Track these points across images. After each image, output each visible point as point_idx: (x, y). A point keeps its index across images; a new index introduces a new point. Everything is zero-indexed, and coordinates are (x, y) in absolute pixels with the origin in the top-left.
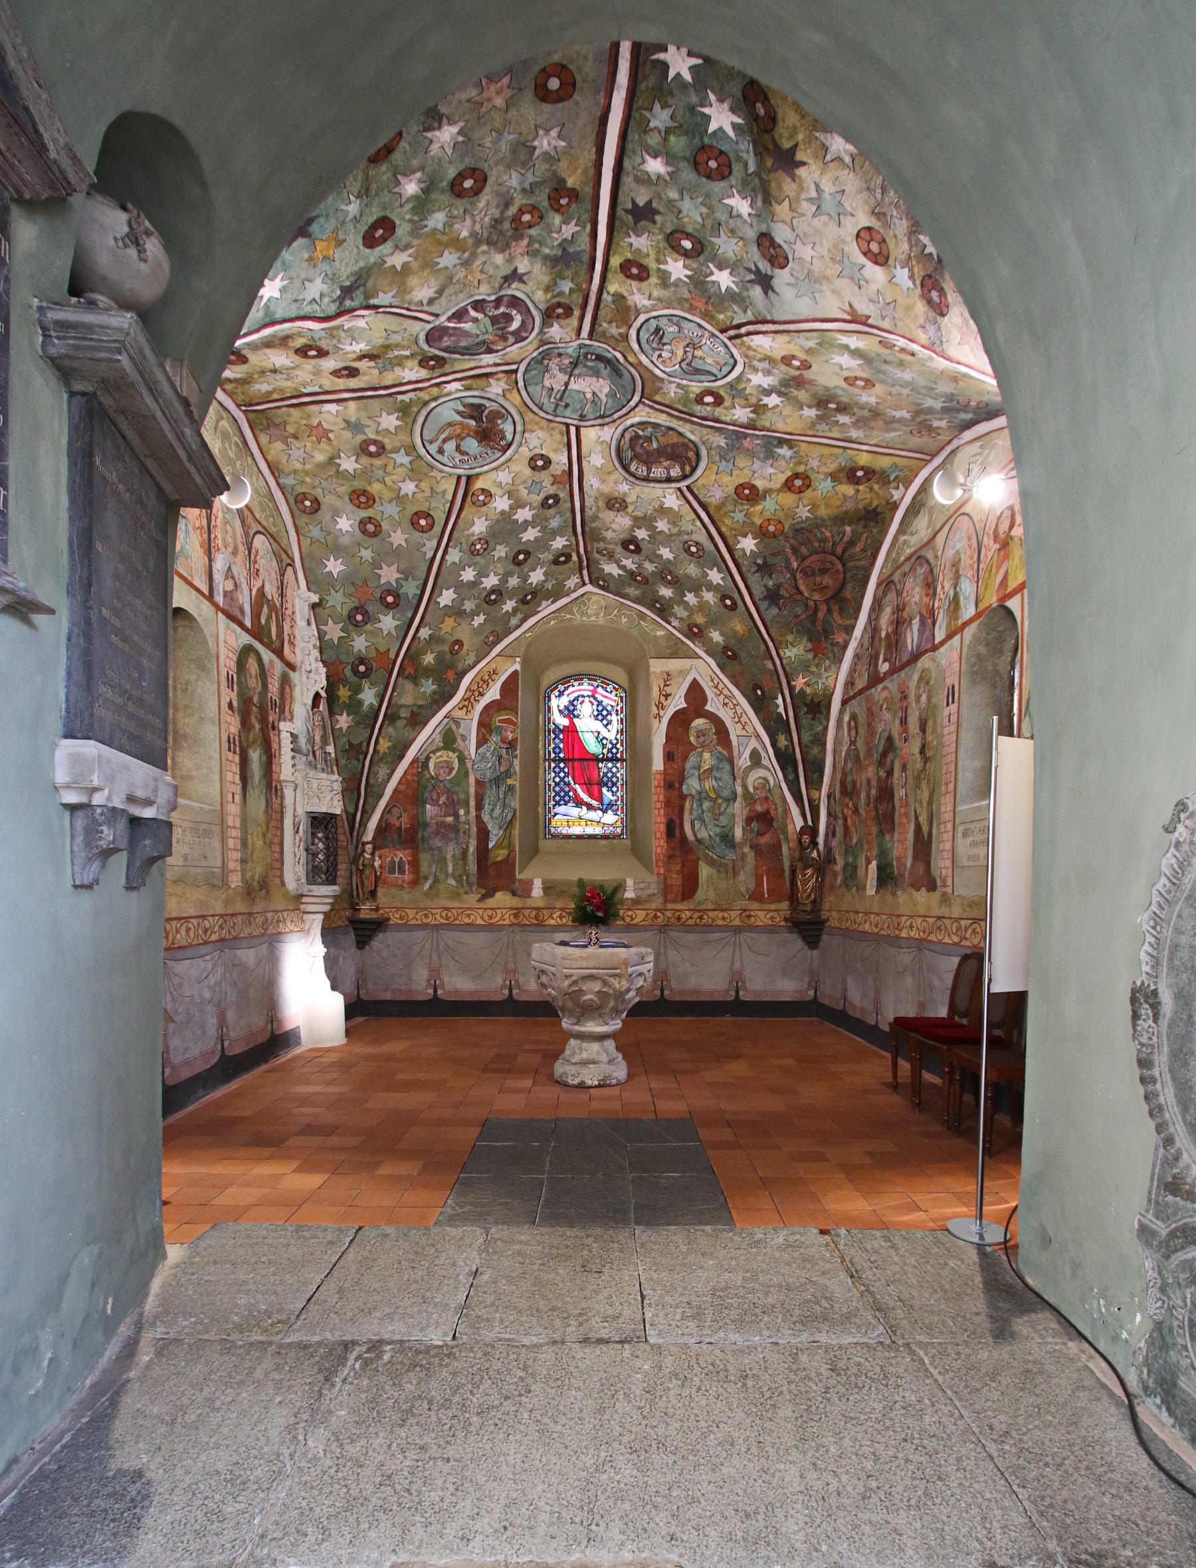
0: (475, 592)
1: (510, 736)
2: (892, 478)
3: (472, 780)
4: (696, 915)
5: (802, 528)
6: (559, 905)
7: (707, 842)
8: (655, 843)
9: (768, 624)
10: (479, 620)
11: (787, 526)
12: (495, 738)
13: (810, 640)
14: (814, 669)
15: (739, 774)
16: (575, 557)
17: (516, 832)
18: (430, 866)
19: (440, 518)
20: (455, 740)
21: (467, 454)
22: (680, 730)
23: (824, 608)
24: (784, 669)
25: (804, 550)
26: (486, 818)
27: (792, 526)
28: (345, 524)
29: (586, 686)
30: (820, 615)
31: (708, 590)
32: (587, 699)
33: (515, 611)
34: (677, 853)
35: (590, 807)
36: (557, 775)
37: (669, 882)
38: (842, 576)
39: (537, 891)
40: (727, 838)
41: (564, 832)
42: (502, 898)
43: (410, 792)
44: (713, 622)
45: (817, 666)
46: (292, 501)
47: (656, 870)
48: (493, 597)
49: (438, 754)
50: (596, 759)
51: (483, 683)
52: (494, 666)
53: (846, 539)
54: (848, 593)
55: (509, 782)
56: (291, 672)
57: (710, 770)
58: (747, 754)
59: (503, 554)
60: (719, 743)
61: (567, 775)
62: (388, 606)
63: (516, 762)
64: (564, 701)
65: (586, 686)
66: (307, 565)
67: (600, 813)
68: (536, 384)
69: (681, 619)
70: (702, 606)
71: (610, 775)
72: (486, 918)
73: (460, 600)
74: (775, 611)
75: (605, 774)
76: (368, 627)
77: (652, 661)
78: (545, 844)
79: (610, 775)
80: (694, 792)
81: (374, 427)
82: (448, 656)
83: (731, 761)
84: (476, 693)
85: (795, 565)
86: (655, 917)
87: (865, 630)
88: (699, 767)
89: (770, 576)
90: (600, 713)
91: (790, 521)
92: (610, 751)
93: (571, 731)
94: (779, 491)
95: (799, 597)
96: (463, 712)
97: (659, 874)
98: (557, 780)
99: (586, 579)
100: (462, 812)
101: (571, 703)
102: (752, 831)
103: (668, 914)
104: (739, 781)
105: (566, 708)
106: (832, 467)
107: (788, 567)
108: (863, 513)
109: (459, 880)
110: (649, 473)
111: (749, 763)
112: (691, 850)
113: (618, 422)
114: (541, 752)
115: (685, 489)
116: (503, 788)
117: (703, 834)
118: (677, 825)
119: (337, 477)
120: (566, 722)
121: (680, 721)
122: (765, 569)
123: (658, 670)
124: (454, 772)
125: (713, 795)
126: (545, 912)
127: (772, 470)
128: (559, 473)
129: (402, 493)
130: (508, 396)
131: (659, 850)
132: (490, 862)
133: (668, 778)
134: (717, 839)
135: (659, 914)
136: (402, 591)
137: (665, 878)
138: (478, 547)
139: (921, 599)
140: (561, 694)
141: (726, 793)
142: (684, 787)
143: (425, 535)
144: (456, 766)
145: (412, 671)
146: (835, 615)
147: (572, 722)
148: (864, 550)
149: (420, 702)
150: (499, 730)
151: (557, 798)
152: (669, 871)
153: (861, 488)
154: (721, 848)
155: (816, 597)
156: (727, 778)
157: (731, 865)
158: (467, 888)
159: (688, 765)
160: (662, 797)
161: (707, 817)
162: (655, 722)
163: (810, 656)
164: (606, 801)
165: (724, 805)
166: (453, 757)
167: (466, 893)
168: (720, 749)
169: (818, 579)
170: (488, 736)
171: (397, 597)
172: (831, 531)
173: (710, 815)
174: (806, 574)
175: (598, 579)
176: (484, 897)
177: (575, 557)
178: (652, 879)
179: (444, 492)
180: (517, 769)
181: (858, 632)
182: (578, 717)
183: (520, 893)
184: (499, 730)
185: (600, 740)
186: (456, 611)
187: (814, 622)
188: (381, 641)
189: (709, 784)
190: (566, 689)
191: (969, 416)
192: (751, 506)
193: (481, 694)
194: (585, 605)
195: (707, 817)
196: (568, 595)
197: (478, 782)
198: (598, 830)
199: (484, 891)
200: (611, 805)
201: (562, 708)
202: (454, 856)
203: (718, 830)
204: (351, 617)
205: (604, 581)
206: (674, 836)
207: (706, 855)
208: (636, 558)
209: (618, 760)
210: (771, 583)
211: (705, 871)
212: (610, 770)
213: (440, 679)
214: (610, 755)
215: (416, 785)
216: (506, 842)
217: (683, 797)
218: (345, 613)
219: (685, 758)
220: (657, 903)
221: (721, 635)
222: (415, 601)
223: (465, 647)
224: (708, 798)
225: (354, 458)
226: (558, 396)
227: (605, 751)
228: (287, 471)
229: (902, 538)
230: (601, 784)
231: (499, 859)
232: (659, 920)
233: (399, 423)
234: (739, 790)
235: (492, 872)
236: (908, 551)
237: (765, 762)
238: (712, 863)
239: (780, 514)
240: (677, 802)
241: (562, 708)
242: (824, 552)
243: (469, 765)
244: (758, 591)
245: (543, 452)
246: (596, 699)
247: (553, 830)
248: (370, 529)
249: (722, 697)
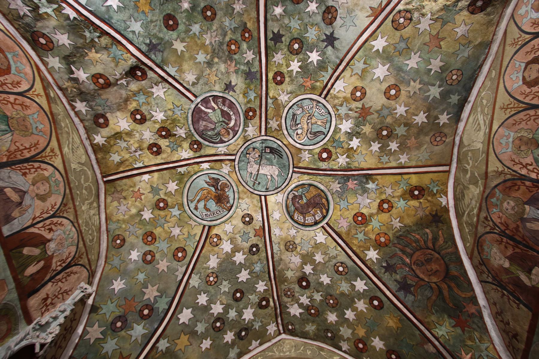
0: (205, 316)
2: (435, 192)
5: (401, 235)
9: (411, 309)
10: (206, 344)
11: (391, 235)
13: (450, 316)
14: (469, 343)
16: (272, 303)
19: (190, 254)
21: (210, 211)
23: (444, 286)
24: (444, 347)
25: (408, 250)
27: (394, 234)
28: (135, 255)
30: (446, 293)
31: (359, 300)
33: (233, 343)
38: (442, 262)
44: (370, 333)
45: (471, 338)
46: (110, 240)
48: (218, 324)
53: (430, 236)
54: (454, 271)
56: (23, 323)
59: (227, 290)
62: (143, 317)
66: (101, 284)
68: (244, 170)
69: (348, 339)
70: (359, 315)
73: (194, 320)
74: (411, 298)
76: (123, 333)
81: (163, 191)
85: (408, 260)
87: (485, 293)
89: (395, 272)
91: (391, 232)
94: (377, 214)
95: (422, 283)
99: (281, 328)
106: (399, 192)
107: (404, 264)
108: (430, 218)
110: (305, 221)
113: (285, 190)
115: (326, 226)
119: (139, 224)
122: (390, 268)
127: (369, 201)
128: (258, 228)
129: (172, 235)
130: (231, 174)
136: (156, 306)
138: (211, 279)
139: (516, 199)
143: (180, 263)
146: (456, 290)
148: (446, 242)
153: (421, 201)
155: (435, 280)
163: (459, 330)
169: (429, 267)
171: (151, 310)
172: (418, 234)
174: (418, 265)
175: (288, 324)
177: (272, 303)
179: (195, 235)
181: (482, 301)
186: (189, 330)
187: (444, 300)
188: (127, 346)
191: (455, 99)
192: (366, 227)
194: (281, 346)
196: (270, 340)
204: (113, 323)
205: (292, 324)
208: (308, 292)
210: (398, 277)
218: (110, 320)
221: (381, 339)
222: (162, 315)
225: (151, 211)
226: (255, 178)
228: (114, 220)
229: (465, 218)
233: (177, 188)
236: (475, 211)
239: (384, 228)
242: (421, 248)
244: (394, 286)
245: (249, 212)
248: (148, 259)
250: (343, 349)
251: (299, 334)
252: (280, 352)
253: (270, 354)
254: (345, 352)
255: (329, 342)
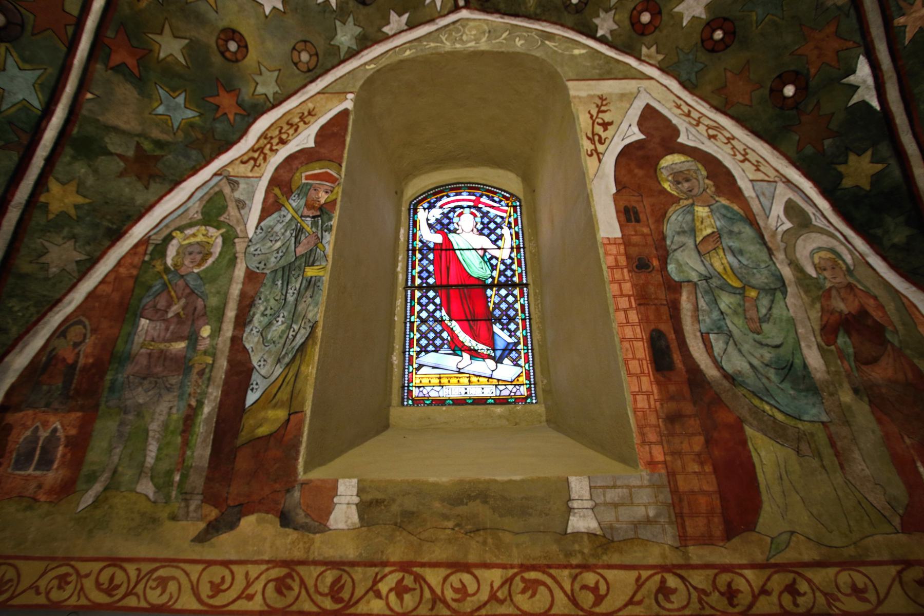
1: (323, 198)
3: (240, 272)
4: (778, 581)
6: (396, 553)
7: (751, 379)
8: (629, 385)
12: (295, 202)
15: (777, 243)
17: (310, 370)
18: (110, 450)
20: (224, 208)
22: (640, 172)
26: (251, 341)
29: (465, 196)
32: (467, 211)
34: (688, 408)
35: (474, 354)
36: (424, 307)
37: (683, 485)
39: (344, 513)
40: (791, 371)
41: (433, 394)
42: (256, 532)
43: (116, 297)
47: (642, 453)
49: (189, 232)
50: (481, 285)
51: (291, 125)
52: (310, 105)
55: (310, 272)
57: (717, 236)
58: (778, 209)
60: (719, 191)
61: (438, 308)
63: (329, 239)
64: (436, 213)
65: (465, 196)
67: (491, 363)
71: (504, 306)
72: (205, 590)
75: (497, 306)
77: (570, 84)
78: (395, 413)
79: (504, 306)
80: (694, 277)
82: (217, 59)
83: (751, 221)
84: (275, 141)
86: (664, 590)
88: (693, 231)
90: (485, 226)
92: (502, 273)
93: (446, 250)
96: (246, 167)
97: (651, 464)
98: (424, 315)
100: (206, 331)
101: (445, 215)
102: (841, 355)
103: (699, 579)
104: (780, 256)
105: (438, 221)
109: (163, 486)
111: (788, 225)
112: (717, 400)
114: (401, 277)
116: (296, 284)
117: (736, 363)
118: (674, 345)
120: (438, 239)
121: (637, 162)
123: (583, 94)
124: (210, 261)
125: (736, 284)
126: (358, 573)
131: (642, 403)
132: (244, 436)
133: (634, 251)
134: (772, 374)
135: (672, 581)
137: (672, 475)
140: (431, 206)
141: (761, 278)
142: (671, 267)
144: (217, 250)
145: (131, 62)
147: (446, 238)
149: (156, 134)
150: (304, 190)
151: (424, 342)
152: (676, 453)
154: (785, 394)
156: (753, 249)
157: (821, 437)
158: (176, 506)
159: (670, 228)
160: (627, 287)
161: (735, 325)
162: (591, 164)
164: (500, 345)
165: (765, 302)
166: (215, 236)
167: (174, 518)
168: (724, 201)
170: (283, 199)
173: (739, 321)
176: (214, 529)
178: (640, 476)
180: (329, 250)
182: (455, 231)
183: (301, 518)
184: (304, 190)
185: (489, 260)
189: (720, 262)
190: (439, 199)
193: (283, 142)
194: (458, 31)
195: (735, 325)
197: (251, 276)
198: (489, 391)
199: (214, 513)
200: (508, 350)
201: (432, 221)
202: (165, 426)
203: (768, 355)
206: (671, 367)
207: (756, 412)
209: (514, 285)
211: (766, 454)
212: (504, 299)
213: (201, 99)
214: (503, 279)
215: (130, 283)
216: (286, 393)
217: (674, 287)
219: (661, 217)
220: (661, 547)
223: (253, 56)
224: (725, 287)
227: (496, 274)
230: (490, 319)
231: (263, 431)
232: (677, 601)
234: (787, 272)
235: (243, 463)
237: (818, 222)
238: (777, 432)
240: (662, 294)
241: (432, 221)
243: (240, 246)
246: (479, 209)
247: (415, 392)
249: (702, 128)
250: (600, 33)
251: (502, 6)
252: (454, 41)
253: (432, 45)
254: (602, 40)
255: (570, 19)
